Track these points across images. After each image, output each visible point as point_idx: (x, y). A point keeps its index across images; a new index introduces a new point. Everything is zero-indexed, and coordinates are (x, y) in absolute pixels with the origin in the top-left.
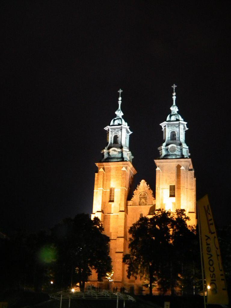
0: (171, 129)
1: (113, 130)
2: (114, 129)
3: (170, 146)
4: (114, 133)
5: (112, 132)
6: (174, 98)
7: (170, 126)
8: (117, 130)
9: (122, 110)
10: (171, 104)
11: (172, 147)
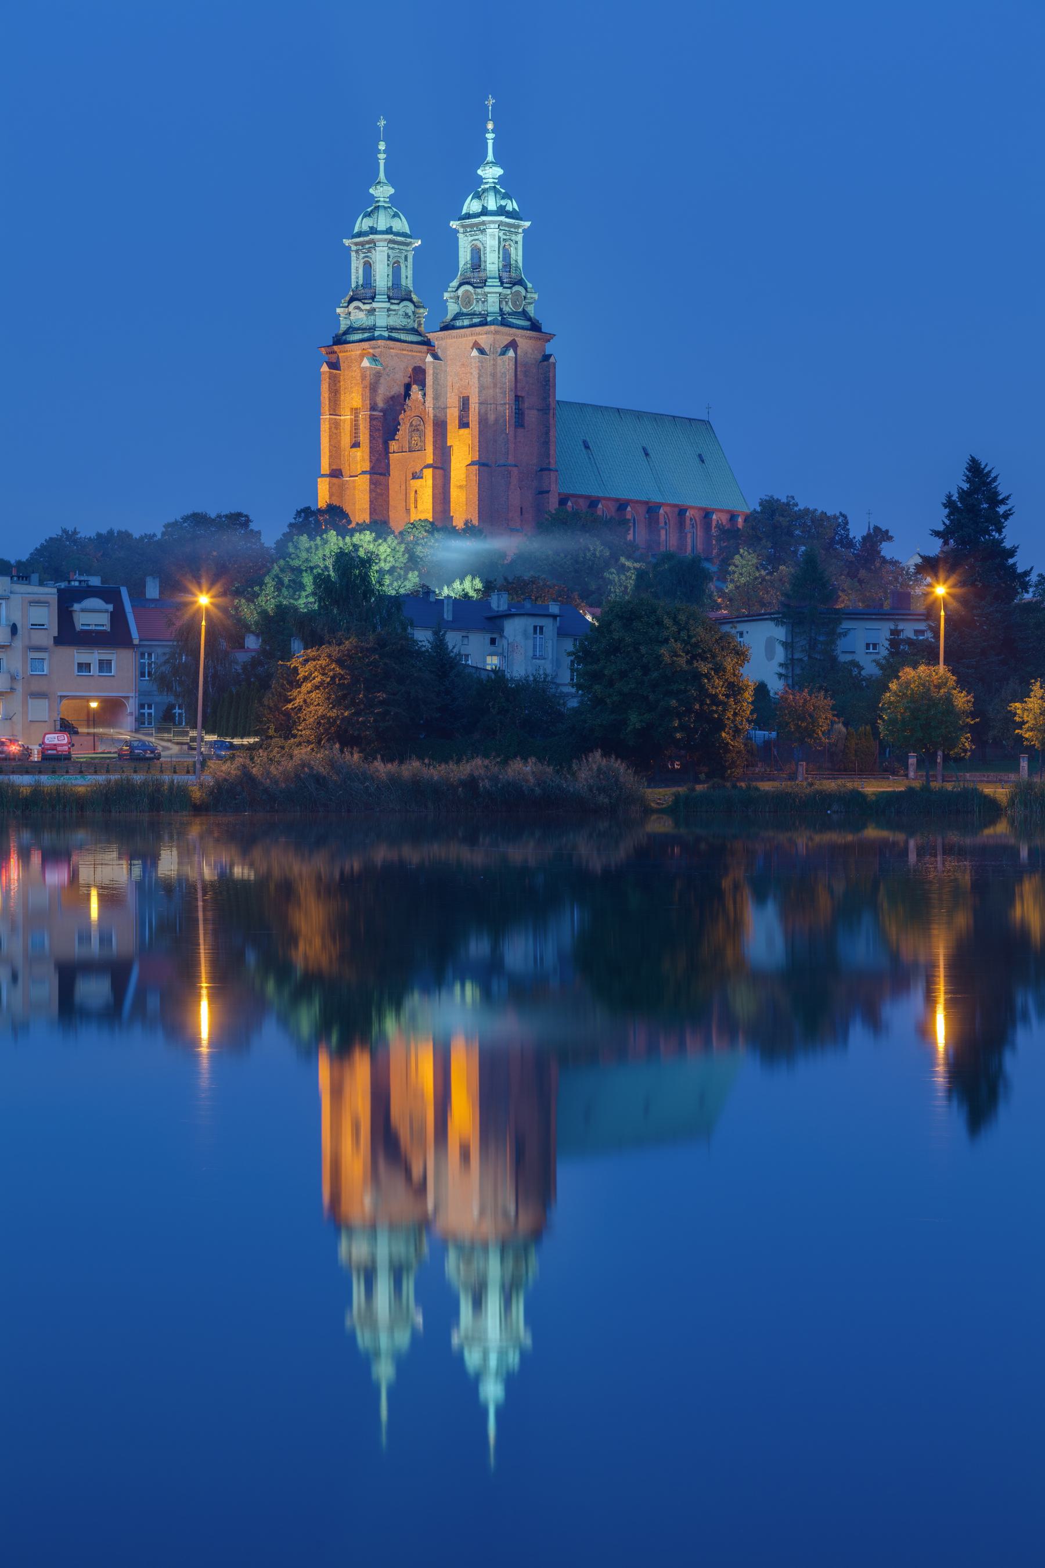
0: (471, 238)
1: (361, 248)
2: (362, 244)
3: (460, 292)
4: (363, 255)
5: (357, 251)
6: (490, 136)
7: (468, 230)
8: (367, 246)
9: (391, 180)
10: (481, 161)
11: (467, 291)
